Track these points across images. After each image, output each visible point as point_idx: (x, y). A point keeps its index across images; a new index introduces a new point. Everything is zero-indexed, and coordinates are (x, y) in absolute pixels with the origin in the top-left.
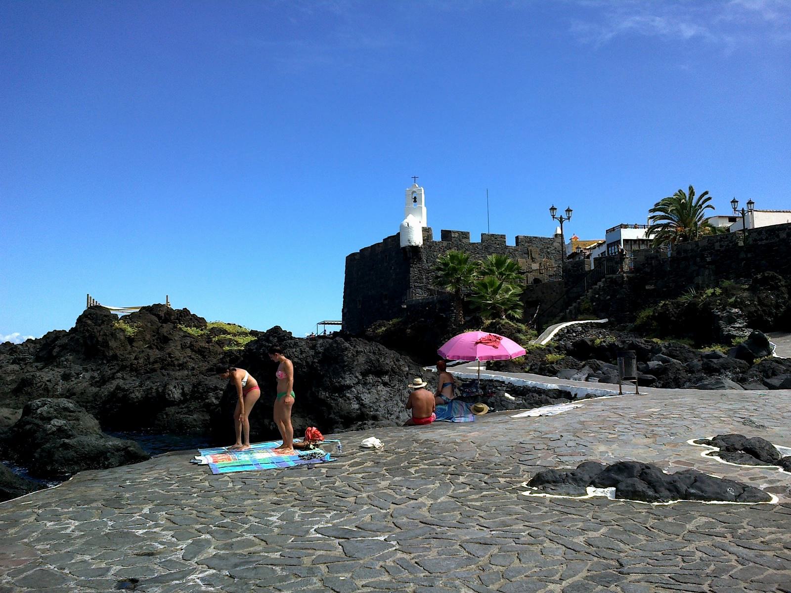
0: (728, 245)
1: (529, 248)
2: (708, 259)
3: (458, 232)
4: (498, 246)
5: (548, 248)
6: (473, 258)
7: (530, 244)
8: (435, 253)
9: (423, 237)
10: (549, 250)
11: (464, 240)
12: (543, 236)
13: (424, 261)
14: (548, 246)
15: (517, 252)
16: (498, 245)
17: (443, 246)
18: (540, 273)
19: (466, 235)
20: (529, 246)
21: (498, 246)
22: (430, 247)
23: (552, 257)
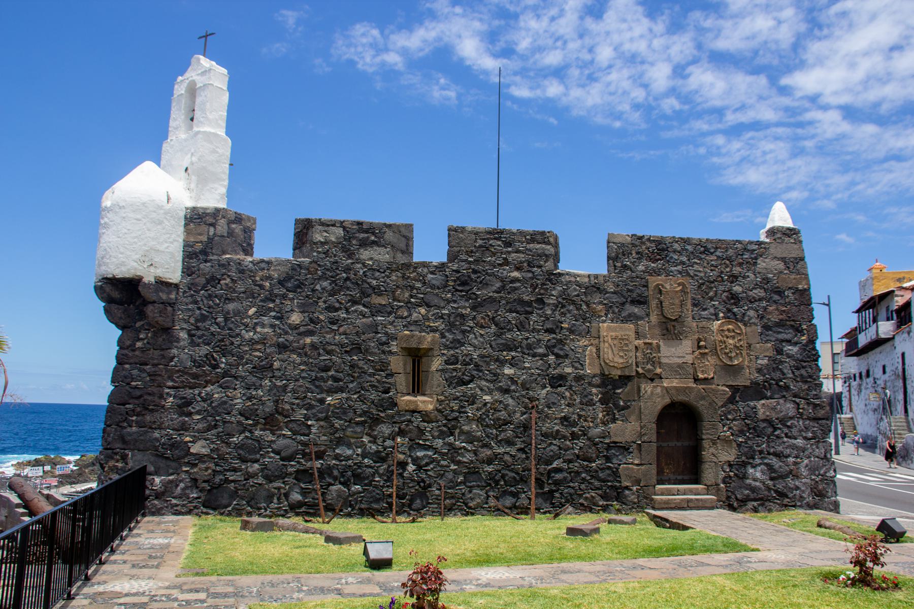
1: (654, 281)
3: (342, 224)
4: (516, 274)
5: (734, 278)
6: (400, 323)
7: (659, 264)
8: (231, 306)
9: (186, 245)
10: (737, 289)
11: (365, 254)
12: (713, 237)
13: (178, 340)
14: (737, 270)
15: (597, 298)
16: (518, 269)
17: (269, 278)
18: (696, 380)
19: (405, 234)
20: (656, 272)
21: (516, 274)
22: (213, 280)
23: (751, 313)
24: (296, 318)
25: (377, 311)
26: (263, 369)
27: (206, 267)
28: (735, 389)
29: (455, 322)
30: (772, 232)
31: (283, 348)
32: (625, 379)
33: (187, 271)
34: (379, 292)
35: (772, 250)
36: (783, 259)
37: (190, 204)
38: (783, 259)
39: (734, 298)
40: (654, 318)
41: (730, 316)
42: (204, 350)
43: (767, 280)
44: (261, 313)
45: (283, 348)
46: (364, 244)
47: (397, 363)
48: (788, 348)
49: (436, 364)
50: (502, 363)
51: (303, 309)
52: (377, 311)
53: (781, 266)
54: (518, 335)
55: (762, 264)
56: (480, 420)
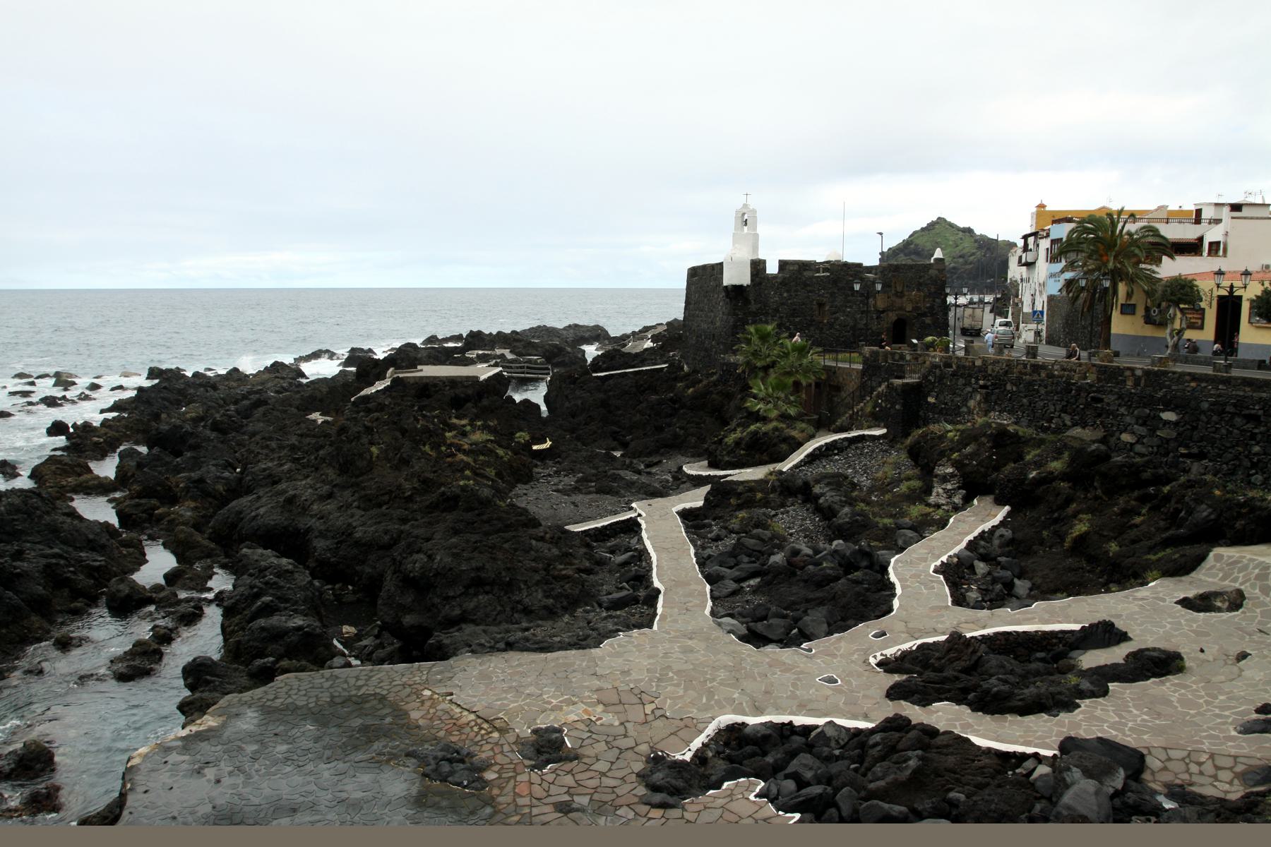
0: (998, 372)
2: (981, 382)
5: (920, 277)
8: (766, 292)
10: (921, 281)
14: (922, 274)
22: (760, 284)
24: (785, 295)
25: (810, 291)
26: (777, 310)
27: (757, 279)
28: (918, 314)
29: (832, 294)
30: (936, 259)
31: (783, 304)
32: (883, 312)
33: (752, 280)
34: (809, 285)
35: (935, 267)
36: (938, 270)
37: (750, 258)
38: (938, 270)
39: (920, 284)
40: (893, 292)
41: (919, 290)
42: (759, 305)
43: (932, 277)
44: (775, 293)
45: (783, 304)
46: (805, 270)
47: (815, 307)
48: (937, 300)
49: (827, 308)
50: (846, 307)
51: (788, 291)
52: (810, 291)
53: (937, 272)
54: (850, 298)
55: (931, 271)
56: (839, 325)
